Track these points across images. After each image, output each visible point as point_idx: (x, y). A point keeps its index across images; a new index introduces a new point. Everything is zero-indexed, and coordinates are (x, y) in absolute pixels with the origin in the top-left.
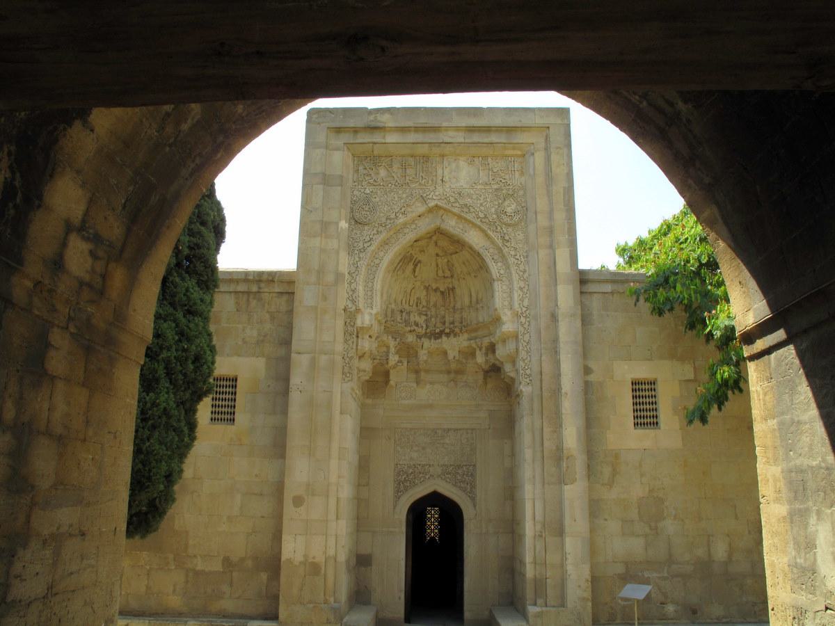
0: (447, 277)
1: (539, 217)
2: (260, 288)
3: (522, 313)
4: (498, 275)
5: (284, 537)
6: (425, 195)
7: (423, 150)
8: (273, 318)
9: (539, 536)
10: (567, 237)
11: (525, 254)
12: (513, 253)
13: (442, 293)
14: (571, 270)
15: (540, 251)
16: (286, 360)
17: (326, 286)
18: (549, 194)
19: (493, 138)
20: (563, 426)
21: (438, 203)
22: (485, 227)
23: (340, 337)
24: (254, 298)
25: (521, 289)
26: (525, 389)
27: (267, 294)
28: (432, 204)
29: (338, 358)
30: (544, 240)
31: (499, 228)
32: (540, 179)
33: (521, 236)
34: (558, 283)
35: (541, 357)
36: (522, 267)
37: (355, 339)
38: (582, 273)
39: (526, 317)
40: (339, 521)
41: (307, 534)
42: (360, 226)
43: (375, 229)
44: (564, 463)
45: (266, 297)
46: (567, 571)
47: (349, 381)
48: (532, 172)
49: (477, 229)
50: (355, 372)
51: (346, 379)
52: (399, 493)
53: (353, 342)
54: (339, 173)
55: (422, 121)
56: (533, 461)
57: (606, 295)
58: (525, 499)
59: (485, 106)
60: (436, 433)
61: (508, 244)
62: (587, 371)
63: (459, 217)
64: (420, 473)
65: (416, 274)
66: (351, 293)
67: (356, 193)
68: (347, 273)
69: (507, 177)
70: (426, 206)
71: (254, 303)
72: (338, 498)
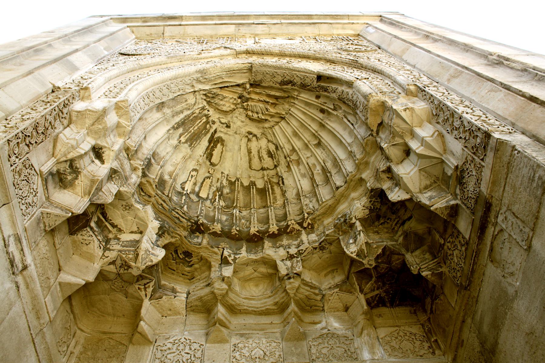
0: (268, 169)
13: (262, 192)
65: (213, 160)
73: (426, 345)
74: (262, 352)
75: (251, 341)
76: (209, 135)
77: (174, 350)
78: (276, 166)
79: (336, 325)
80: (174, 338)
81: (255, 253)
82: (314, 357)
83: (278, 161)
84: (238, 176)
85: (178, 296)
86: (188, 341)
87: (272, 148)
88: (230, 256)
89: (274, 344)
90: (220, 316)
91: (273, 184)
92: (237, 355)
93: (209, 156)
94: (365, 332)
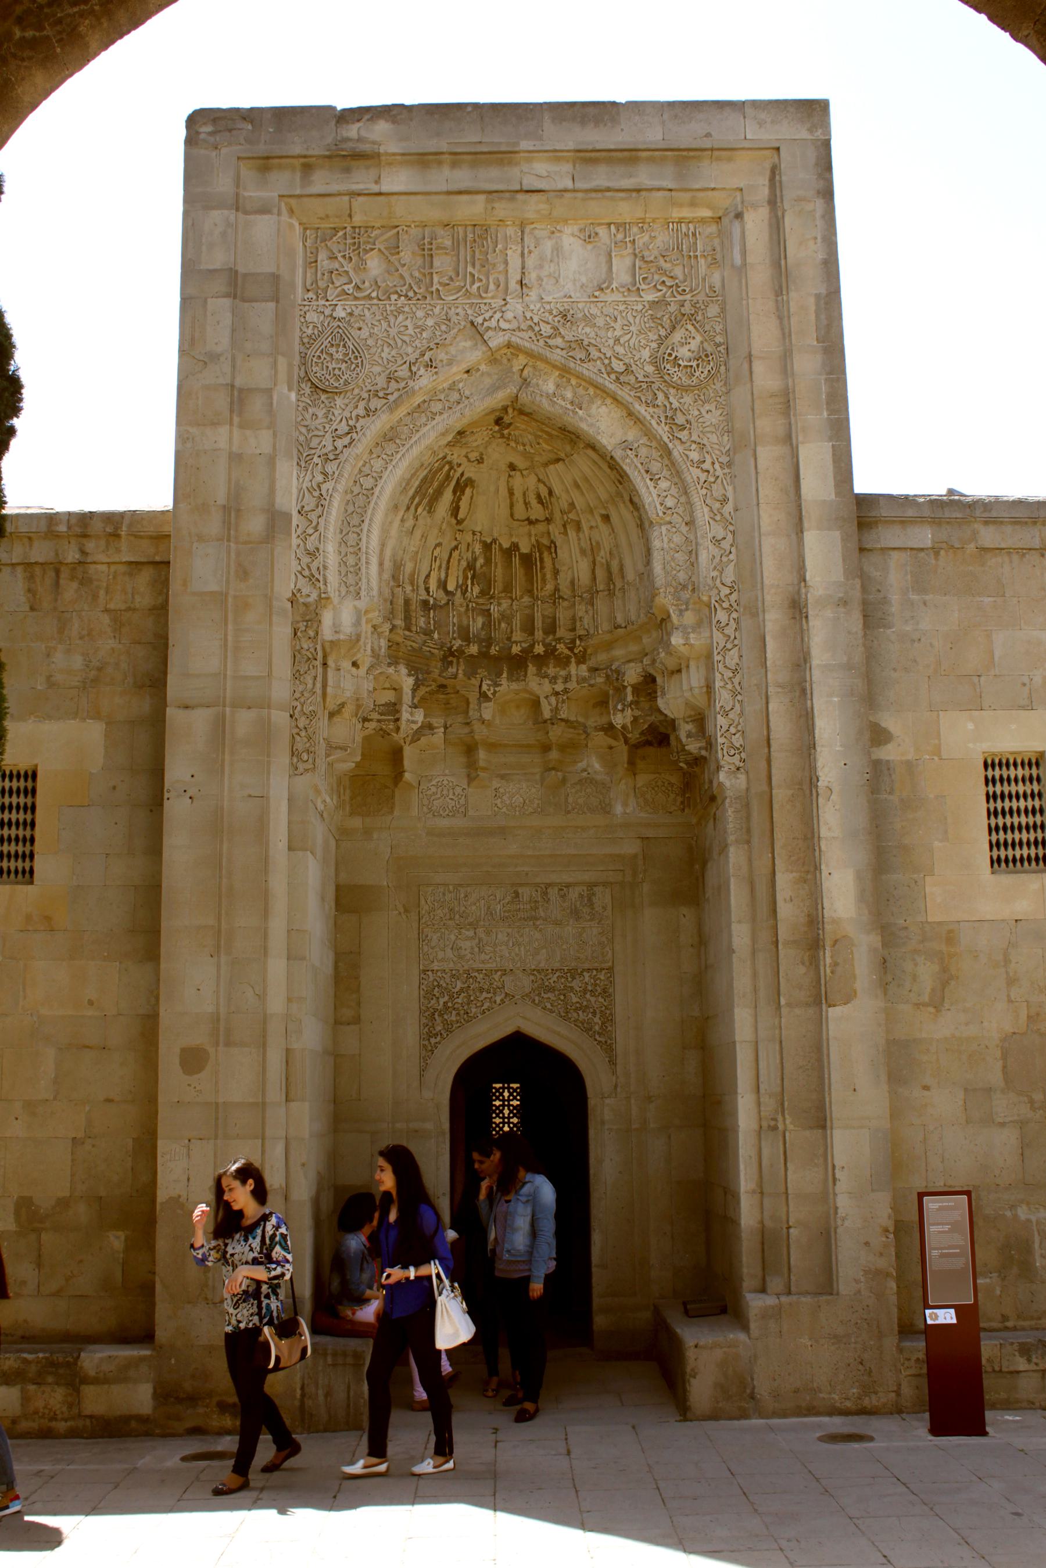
0: (537, 520)
1: (758, 367)
2: (83, 552)
3: (720, 601)
4: (660, 510)
5: (162, 1145)
6: (480, 320)
7: (473, 209)
8: (118, 623)
9: (768, 1128)
10: (825, 414)
11: (725, 459)
12: (695, 456)
13: (527, 561)
14: (837, 494)
15: (759, 449)
16: (156, 726)
17: (246, 543)
18: (782, 315)
19: (643, 176)
20: (823, 867)
21: (513, 339)
22: (624, 394)
23: (283, 666)
24: (72, 578)
25: (717, 542)
26: (729, 780)
27: (104, 568)
28: (496, 341)
29: (280, 718)
30: (768, 424)
31: (661, 396)
32: (760, 276)
33: (713, 417)
34: (806, 525)
35: (767, 703)
36: (717, 491)
37: (320, 670)
38: (866, 502)
39: (729, 610)
40: (293, 1105)
41: (216, 1137)
42: (323, 397)
43: (362, 405)
44: (828, 954)
45: (100, 571)
46: (836, 1208)
47: (307, 770)
48: (738, 261)
49: (609, 401)
50: (321, 749)
51: (301, 767)
52: (431, 1038)
53: (315, 678)
54: (270, 269)
55: (470, 137)
56: (754, 953)
57: (922, 554)
58: (734, 1043)
59: (621, 99)
60: (517, 894)
61: (684, 435)
62: (879, 736)
63: (565, 371)
64: (481, 990)
65: (460, 516)
66: (306, 560)
67: (312, 317)
68: (295, 513)
69: (678, 272)
70: (484, 349)
71: (70, 590)
72: (287, 1050)
73: (680, 799)
76: (453, 483)
78: (548, 520)
79: (597, 766)
81: (517, 680)
83: (552, 514)
84: (496, 535)
87: (544, 492)
88: (489, 690)
89: (534, 790)
91: (544, 549)
93: (455, 510)
94: (623, 781)
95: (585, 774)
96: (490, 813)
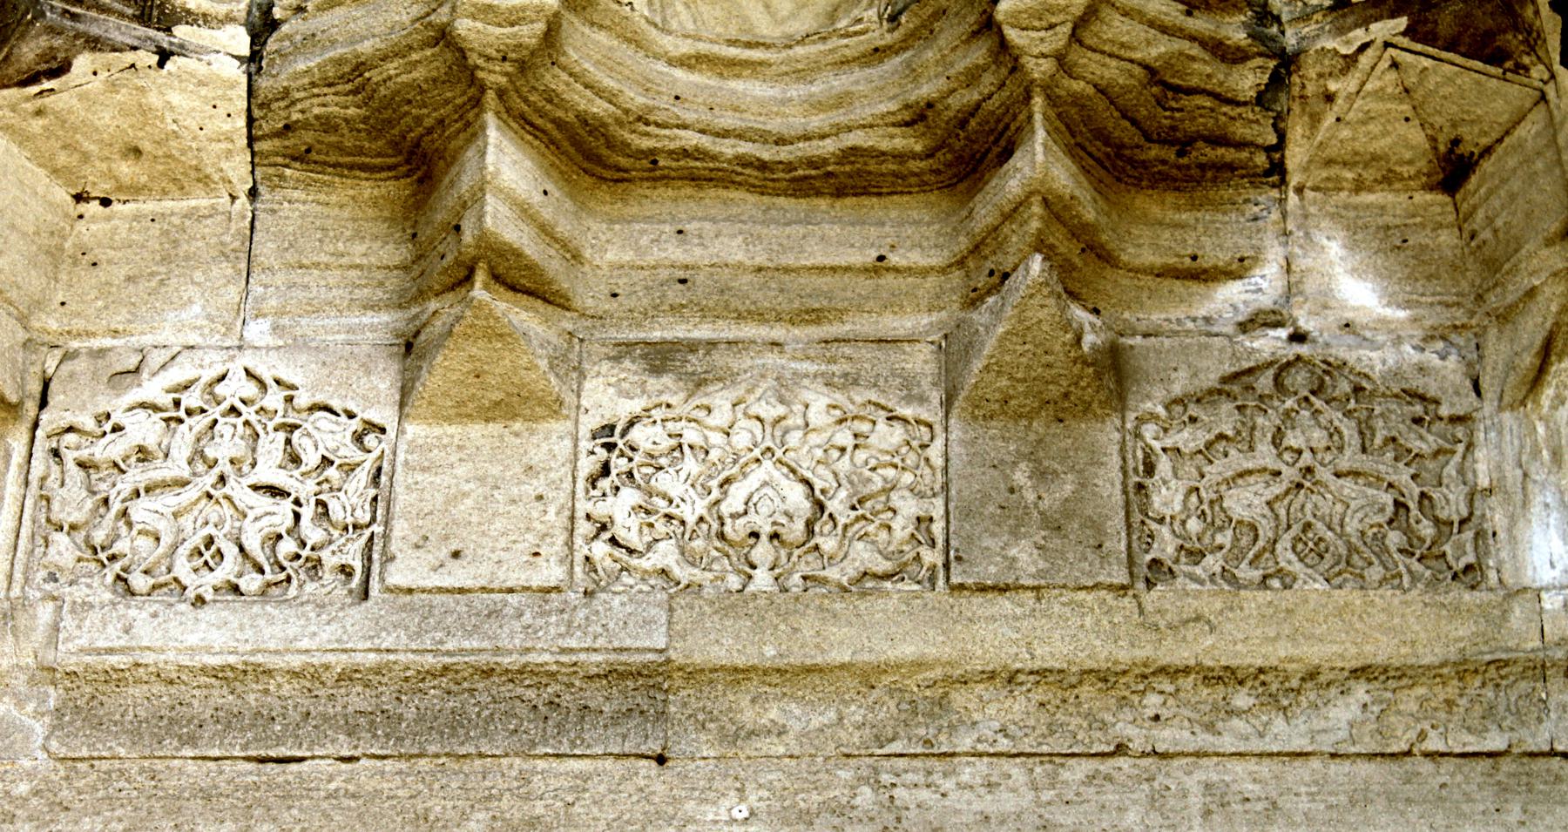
74: (796, 496)
75: (721, 400)
77: (177, 467)
80: (176, 375)
82: (1165, 545)
85: (183, 50)
86: (274, 399)
89: (888, 436)
90: (500, 222)
92: (621, 507)
95: (1270, 343)
96: (550, 572)
